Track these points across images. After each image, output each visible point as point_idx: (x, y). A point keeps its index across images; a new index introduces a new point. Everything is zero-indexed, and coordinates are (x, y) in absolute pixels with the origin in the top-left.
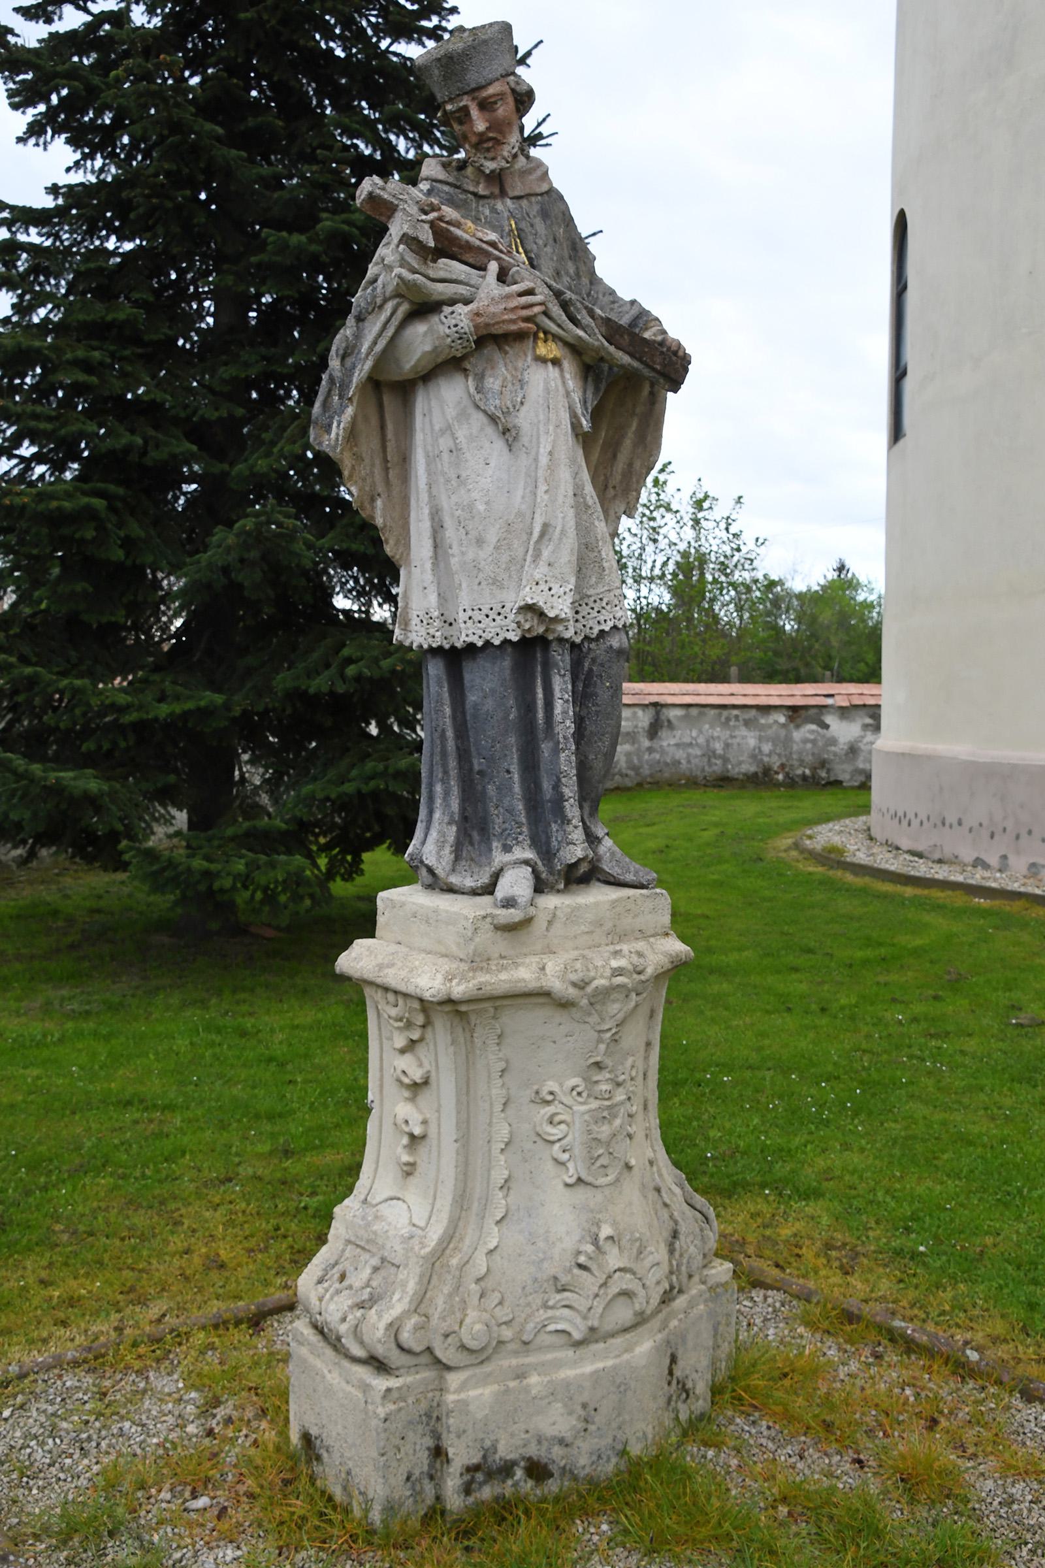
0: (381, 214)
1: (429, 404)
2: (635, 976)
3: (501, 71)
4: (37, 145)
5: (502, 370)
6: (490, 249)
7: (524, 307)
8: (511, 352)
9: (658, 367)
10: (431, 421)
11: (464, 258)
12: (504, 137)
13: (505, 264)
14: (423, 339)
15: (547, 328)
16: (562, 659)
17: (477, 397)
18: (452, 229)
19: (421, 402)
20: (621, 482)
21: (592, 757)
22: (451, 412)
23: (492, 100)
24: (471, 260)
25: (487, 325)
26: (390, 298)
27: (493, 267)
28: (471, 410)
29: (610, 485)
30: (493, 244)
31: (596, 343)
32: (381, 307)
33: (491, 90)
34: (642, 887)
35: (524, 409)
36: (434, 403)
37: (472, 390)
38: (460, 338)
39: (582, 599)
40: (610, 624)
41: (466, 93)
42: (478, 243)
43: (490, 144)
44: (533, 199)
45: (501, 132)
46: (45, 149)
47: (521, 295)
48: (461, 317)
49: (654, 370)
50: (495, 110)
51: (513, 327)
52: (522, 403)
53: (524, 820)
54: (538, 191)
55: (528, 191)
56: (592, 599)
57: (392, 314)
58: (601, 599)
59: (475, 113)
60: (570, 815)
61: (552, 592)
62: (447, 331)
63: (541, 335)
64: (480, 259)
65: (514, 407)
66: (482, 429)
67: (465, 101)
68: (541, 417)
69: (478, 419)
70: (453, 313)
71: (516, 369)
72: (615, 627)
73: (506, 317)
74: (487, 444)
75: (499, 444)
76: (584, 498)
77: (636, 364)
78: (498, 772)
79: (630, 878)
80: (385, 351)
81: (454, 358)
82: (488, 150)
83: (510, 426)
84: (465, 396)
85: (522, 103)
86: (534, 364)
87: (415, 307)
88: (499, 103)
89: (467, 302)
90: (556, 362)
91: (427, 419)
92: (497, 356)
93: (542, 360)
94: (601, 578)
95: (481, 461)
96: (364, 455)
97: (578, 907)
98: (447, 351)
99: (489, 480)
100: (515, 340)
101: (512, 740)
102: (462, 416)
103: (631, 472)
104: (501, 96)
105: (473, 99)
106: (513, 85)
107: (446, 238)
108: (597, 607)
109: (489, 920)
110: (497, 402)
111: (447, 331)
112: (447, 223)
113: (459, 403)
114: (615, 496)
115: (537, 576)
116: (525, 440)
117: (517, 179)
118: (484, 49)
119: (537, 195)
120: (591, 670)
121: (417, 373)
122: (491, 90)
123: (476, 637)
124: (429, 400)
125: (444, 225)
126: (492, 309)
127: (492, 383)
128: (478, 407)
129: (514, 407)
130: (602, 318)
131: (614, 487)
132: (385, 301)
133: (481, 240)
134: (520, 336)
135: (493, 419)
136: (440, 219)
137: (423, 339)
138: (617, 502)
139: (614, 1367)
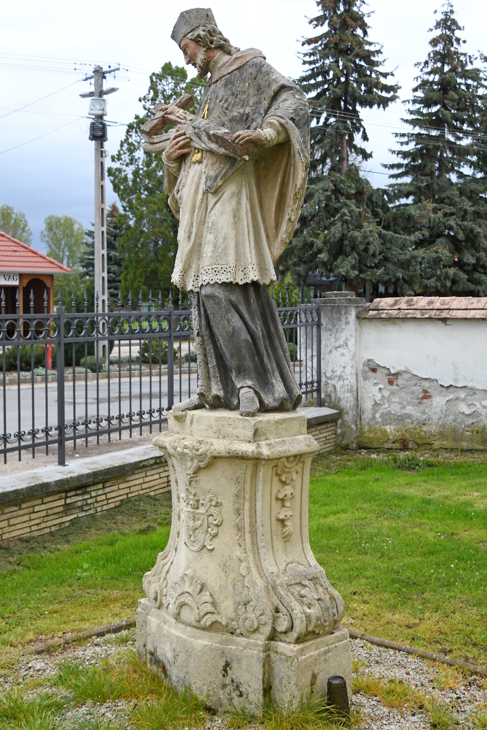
2: (194, 451)
3: (182, 35)
35: (185, 188)
44: (223, 79)
54: (225, 73)
55: (220, 76)
106: (190, 38)
139: (184, 640)
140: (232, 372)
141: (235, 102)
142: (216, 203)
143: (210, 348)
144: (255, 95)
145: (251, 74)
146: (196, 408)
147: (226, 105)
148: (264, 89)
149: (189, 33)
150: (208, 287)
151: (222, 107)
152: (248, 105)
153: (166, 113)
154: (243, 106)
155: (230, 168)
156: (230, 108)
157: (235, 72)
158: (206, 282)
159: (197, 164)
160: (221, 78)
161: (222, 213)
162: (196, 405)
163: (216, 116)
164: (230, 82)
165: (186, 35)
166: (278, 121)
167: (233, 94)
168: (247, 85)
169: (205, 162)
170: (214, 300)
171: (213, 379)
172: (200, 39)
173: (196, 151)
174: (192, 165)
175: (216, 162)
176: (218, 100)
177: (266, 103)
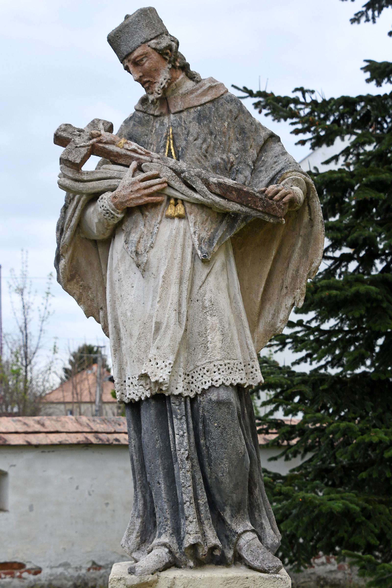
3: (141, 40)
4: (368, 20)
5: (141, 227)
6: (133, 154)
7: (145, 188)
8: (149, 215)
9: (261, 209)
11: (119, 162)
12: (154, 79)
15: (175, 197)
16: (178, 408)
18: (107, 146)
20: (291, 283)
21: (220, 474)
23: (138, 59)
24: (123, 163)
29: (284, 286)
30: (134, 151)
31: (209, 201)
33: (136, 54)
34: (264, 571)
35: (153, 251)
39: (195, 368)
40: (209, 384)
42: (124, 151)
44: (192, 110)
45: (151, 76)
46: (374, 22)
47: (143, 181)
49: (259, 211)
50: (143, 65)
51: (141, 201)
53: (168, 516)
54: (196, 104)
55: (187, 106)
56: (199, 368)
58: (204, 368)
60: (187, 513)
61: (158, 366)
66: (130, 266)
70: (102, 198)
71: (150, 226)
72: (212, 386)
73: (133, 196)
74: (132, 275)
75: (138, 274)
76: (203, 302)
77: (245, 209)
78: (154, 483)
79: (257, 564)
87: (91, 197)
88: (145, 60)
89: (112, 190)
90: (180, 217)
93: (172, 218)
94: (205, 353)
95: (129, 285)
96: (91, 285)
97: (194, 580)
99: (133, 297)
100: (152, 207)
101: (159, 462)
103: (297, 276)
104: (146, 55)
106: (154, 46)
107: (105, 153)
108: (201, 373)
109: (122, 582)
112: (106, 143)
114: (286, 294)
115: (150, 356)
116: (154, 270)
117: (179, 100)
118: (127, 30)
119: (196, 107)
120: (204, 416)
122: (136, 54)
123: (135, 395)
125: (101, 145)
130: (215, 184)
131: (286, 287)
133: (127, 150)
134: (155, 205)
136: (100, 142)
138: (287, 297)
140: (224, 510)
141: (215, 144)
142: (208, 275)
143: (199, 476)
144: (237, 139)
145: (231, 111)
146: (166, 567)
147: (204, 146)
148: (249, 134)
149: (152, 39)
150: (221, 390)
151: (201, 148)
152: (229, 151)
153: (100, 142)
154: (224, 151)
155: (227, 231)
156: (210, 150)
157: (208, 105)
158: (220, 382)
159: (176, 220)
160: (188, 109)
161: (218, 289)
162: (167, 563)
163: (194, 158)
164: (205, 118)
165: (147, 41)
166: (305, 179)
167: (211, 134)
168: (226, 124)
169: (191, 218)
170: (228, 408)
171: (206, 522)
172: (168, 51)
173: (172, 201)
174: (164, 220)
175: (207, 220)
176: (191, 138)
177: (253, 152)
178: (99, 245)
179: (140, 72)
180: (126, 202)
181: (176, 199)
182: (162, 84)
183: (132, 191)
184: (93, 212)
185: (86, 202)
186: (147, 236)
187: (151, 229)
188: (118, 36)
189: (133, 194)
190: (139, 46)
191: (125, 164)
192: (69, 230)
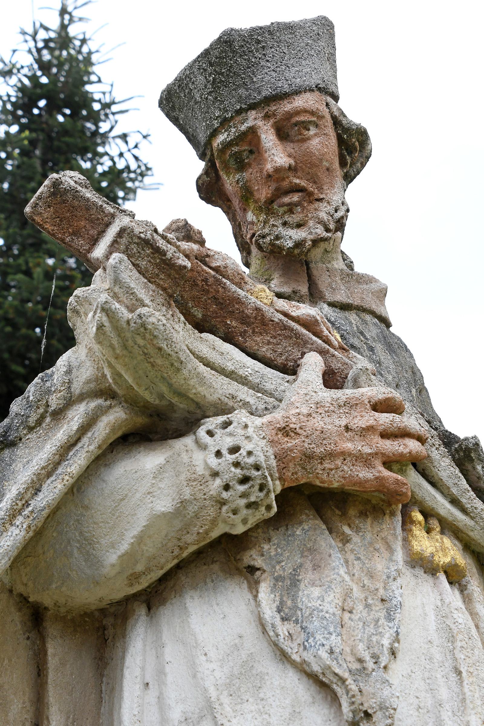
0: (76, 233)
1: (159, 657)
8: (356, 539)
10: (160, 698)
12: (320, 189)
13: (335, 365)
14: (153, 488)
15: (430, 503)
17: (283, 629)
19: (140, 653)
22: (214, 673)
23: (302, 118)
24: (265, 351)
25: (309, 456)
26: (81, 398)
27: (312, 365)
28: (269, 666)
32: (58, 414)
36: (170, 652)
37: (269, 612)
38: (245, 480)
41: (253, 107)
43: (295, 198)
48: (250, 435)
50: (305, 140)
52: (393, 653)
57: (85, 429)
59: (268, 138)
62: (213, 462)
63: (418, 517)
64: (285, 351)
65: (376, 658)
67: (253, 119)
68: (444, 693)
69: (286, 688)
71: (371, 575)
73: (349, 446)
80: (56, 511)
81: (227, 537)
82: (291, 208)
83: (370, 704)
84: (250, 630)
85: (351, 150)
86: (408, 572)
87: (141, 420)
88: (313, 131)
91: (152, 695)
92: (326, 542)
98: (212, 512)
100: (363, 514)
102: (243, 679)
105: (267, 117)
110: (334, 640)
111: (213, 462)
113: (236, 647)
121: (135, 577)
124: (159, 646)
126: (318, 422)
127: (319, 596)
128: (283, 656)
129: (376, 658)
132: (70, 402)
133: (286, 315)
135: (324, 685)
137: (153, 488)
178: (52, 630)
179: (290, 156)
180: (322, 459)
181: (427, 514)
182: (336, 211)
183: (347, 428)
184: (161, 469)
185: (119, 434)
186: (367, 606)
187: (380, 585)
188: (258, 42)
189: (350, 440)
190: (311, 90)
191: (269, 354)
192: (19, 520)
